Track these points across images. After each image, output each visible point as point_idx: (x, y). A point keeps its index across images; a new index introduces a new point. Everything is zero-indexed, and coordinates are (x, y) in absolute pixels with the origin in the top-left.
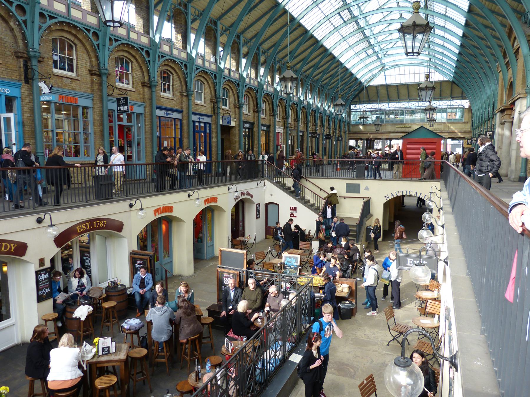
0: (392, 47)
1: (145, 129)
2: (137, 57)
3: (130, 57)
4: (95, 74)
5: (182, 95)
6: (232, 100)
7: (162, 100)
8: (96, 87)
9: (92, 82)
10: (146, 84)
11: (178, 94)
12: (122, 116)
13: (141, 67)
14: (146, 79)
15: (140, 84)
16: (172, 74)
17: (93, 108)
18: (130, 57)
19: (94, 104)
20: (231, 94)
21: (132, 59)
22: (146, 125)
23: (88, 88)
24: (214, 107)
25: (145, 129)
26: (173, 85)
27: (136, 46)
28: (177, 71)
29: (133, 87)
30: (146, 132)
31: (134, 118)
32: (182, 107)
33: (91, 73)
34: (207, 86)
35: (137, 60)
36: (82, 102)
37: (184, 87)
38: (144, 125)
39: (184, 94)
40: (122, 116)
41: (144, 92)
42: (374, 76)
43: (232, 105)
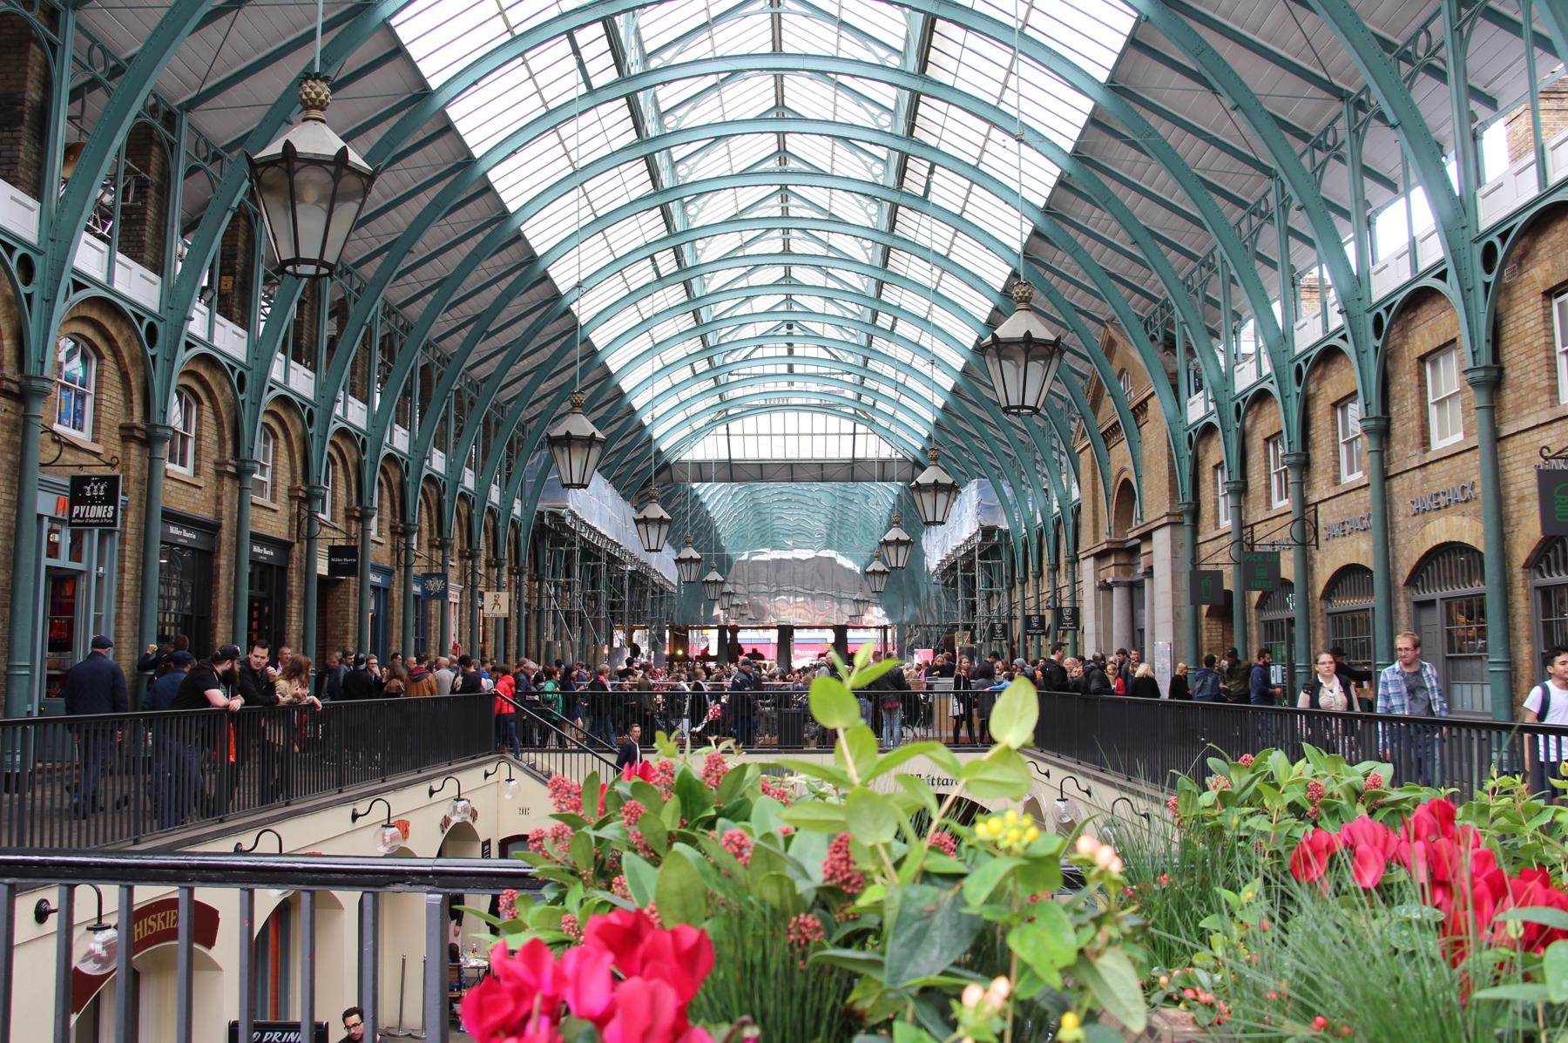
0: (745, 359)
1: (120, 585)
2: (120, 343)
3: (98, 341)
5: (220, 474)
6: (342, 491)
10: (137, 433)
11: (208, 467)
13: (125, 378)
14: (137, 418)
15: (116, 430)
18: (98, 341)
20: (340, 475)
21: (104, 349)
22: (122, 570)
24: (299, 514)
25: (120, 585)
26: (198, 437)
27: (127, 307)
28: (217, 392)
29: (95, 440)
30: (121, 594)
32: (218, 513)
34: (282, 444)
35: (116, 353)
37: (229, 446)
38: (116, 570)
39: (231, 469)
42: (696, 434)
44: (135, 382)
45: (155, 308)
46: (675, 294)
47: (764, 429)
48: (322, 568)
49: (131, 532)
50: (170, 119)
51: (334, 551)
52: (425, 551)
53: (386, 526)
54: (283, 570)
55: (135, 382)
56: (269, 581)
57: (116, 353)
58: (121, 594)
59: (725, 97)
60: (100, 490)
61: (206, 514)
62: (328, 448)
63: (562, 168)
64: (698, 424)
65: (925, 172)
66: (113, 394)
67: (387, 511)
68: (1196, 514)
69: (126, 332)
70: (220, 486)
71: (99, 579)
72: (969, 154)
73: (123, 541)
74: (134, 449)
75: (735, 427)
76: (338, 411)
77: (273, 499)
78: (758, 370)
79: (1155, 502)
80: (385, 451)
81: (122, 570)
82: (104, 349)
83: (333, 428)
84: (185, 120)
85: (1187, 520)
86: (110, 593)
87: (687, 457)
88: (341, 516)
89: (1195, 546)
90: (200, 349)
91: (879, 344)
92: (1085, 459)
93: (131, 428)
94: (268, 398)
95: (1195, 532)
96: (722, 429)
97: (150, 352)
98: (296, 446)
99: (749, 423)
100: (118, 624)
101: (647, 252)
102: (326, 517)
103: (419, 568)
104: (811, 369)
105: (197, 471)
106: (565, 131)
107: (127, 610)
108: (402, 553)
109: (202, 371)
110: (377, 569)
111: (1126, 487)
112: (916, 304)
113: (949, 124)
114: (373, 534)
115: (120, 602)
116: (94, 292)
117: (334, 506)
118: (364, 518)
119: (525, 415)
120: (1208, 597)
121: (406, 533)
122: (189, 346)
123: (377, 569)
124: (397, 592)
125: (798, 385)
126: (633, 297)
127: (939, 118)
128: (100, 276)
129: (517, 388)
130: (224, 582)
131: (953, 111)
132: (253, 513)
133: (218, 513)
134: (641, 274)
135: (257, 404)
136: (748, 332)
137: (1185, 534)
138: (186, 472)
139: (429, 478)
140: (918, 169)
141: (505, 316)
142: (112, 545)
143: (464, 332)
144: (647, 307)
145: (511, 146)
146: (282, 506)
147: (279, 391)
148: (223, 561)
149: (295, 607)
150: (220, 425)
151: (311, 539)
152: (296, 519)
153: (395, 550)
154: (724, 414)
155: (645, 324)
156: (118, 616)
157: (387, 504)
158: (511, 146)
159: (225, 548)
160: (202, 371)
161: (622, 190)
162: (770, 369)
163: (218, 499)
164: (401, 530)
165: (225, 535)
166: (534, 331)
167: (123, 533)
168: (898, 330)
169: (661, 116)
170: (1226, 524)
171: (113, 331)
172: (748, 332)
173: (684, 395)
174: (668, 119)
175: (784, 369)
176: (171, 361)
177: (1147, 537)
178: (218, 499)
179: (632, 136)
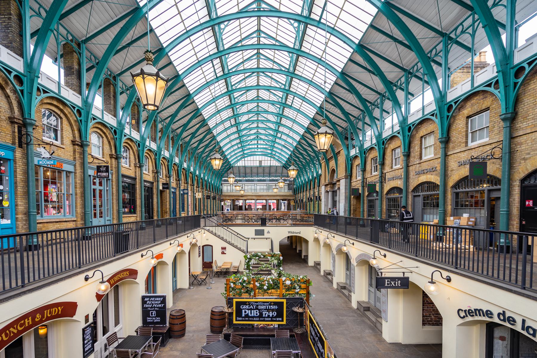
2: (107, 134)
4: (78, 145)
5: (135, 167)
7: (123, 169)
8: (77, 156)
9: (74, 151)
11: (132, 165)
12: (95, 181)
13: (109, 142)
16: (129, 150)
17: (75, 173)
19: (75, 170)
23: (71, 155)
25: (112, 192)
31: (104, 182)
32: (136, 175)
33: (74, 143)
35: (107, 137)
36: (67, 167)
40: (95, 181)
41: (111, 162)
42: (238, 161)
43: (164, 175)
44: (112, 144)
45: (116, 126)
46: (234, 129)
47: (252, 159)
48: (161, 188)
49: (114, 179)
50: (115, 78)
51: (163, 184)
52: (183, 184)
53: (174, 179)
54: (152, 188)
55: (112, 144)
56: (149, 191)
57: (107, 137)
58: (113, 194)
59: (246, 82)
60: (104, 169)
61: (133, 176)
62: (161, 161)
63: (210, 98)
64: (239, 158)
65: (292, 99)
66: (107, 147)
67: (174, 176)
68: (351, 176)
69: (109, 131)
70: (136, 169)
71: (107, 190)
72: (303, 93)
73: (112, 182)
74: (113, 160)
75: (246, 159)
76: (162, 153)
77: (149, 172)
78: (251, 147)
79: (341, 172)
80: (173, 162)
81: (113, 188)
82: (103, 135)
83: (161, 157)
84: (119, 78)
85: (349, 177)
86: (110, 193)
87: (236, 165)
88: (164, 176)
89: (351, 183)
90: (128, 137)
91: (277, 140)
92: (323, 165)
93: (113, 155)
94: (146, 149)
95: (351, 180)
96: (243, 159)
97: (115, 137)
98: (153, 161)
99: (249, 158)
100: (113, 201)
101: (229, 119)
102: (161, 177)
103: (182, 188)
104: (262, 146)
105: (130, 166)
106: (211, 88)
107: (115, 197)
108: (178, 185)
109: (129, 142)
110: (173, 188)
111: (333, 171)
112: (286, 131)
113: (299, 86)
114: (172, 181)
115: (113, 196)
116: (99, 120)
117: (163, 174)
118: (169, 177)
119: (203, 156)
120: (355, 195)
121: (179, 180)
122: (125, 136)
123: (173, 188)
124: (177, 193)
125: (259, 150)
126: (226, 130)
127: (297, 85)
128: (101, 117)
129: (201, 150)
130: (138, 191)
131: (301, 83)
132: (144, 176)
133: (136, 175)
134: (227, 124)
135: (143, 151)
136: (249, 138)
137: (349, 180)
138: (127, 166)
139: (183, 169)
140: (290, 97)
141: (198, 133)
142: (110, 183)
143: (190, 137)
144: (229, 132)
145: (199, 91)
146: (151, 174)
147: (148, 148)
148: (137, 186)
149: (155, 196)
150: (135, 155)
151: (158, 181)
152: (154, 177)
153: (177, 184)
154: (243, 156)
155: (228, 136)
156: (113, 199)
157: (174, 174)
158: (199, 91)
159: (138, 183)
160: (129, 142)
161: (224, 104)
162: (253, 146)
163: (135, 172)
164: (178, 180)
165: (137, 180)
166: (204, 137)
167: (112, 180)
168: (282, 137)
169: (232, 86)
170: (359, 178)
171: (105, 131)
172: (249, 138)
173: (236, 152)
174: (234, 87)
175: (256, 146)
176: (121, 139)
177: (339, 181)
178: (135, 172)
179: (226, 90)
